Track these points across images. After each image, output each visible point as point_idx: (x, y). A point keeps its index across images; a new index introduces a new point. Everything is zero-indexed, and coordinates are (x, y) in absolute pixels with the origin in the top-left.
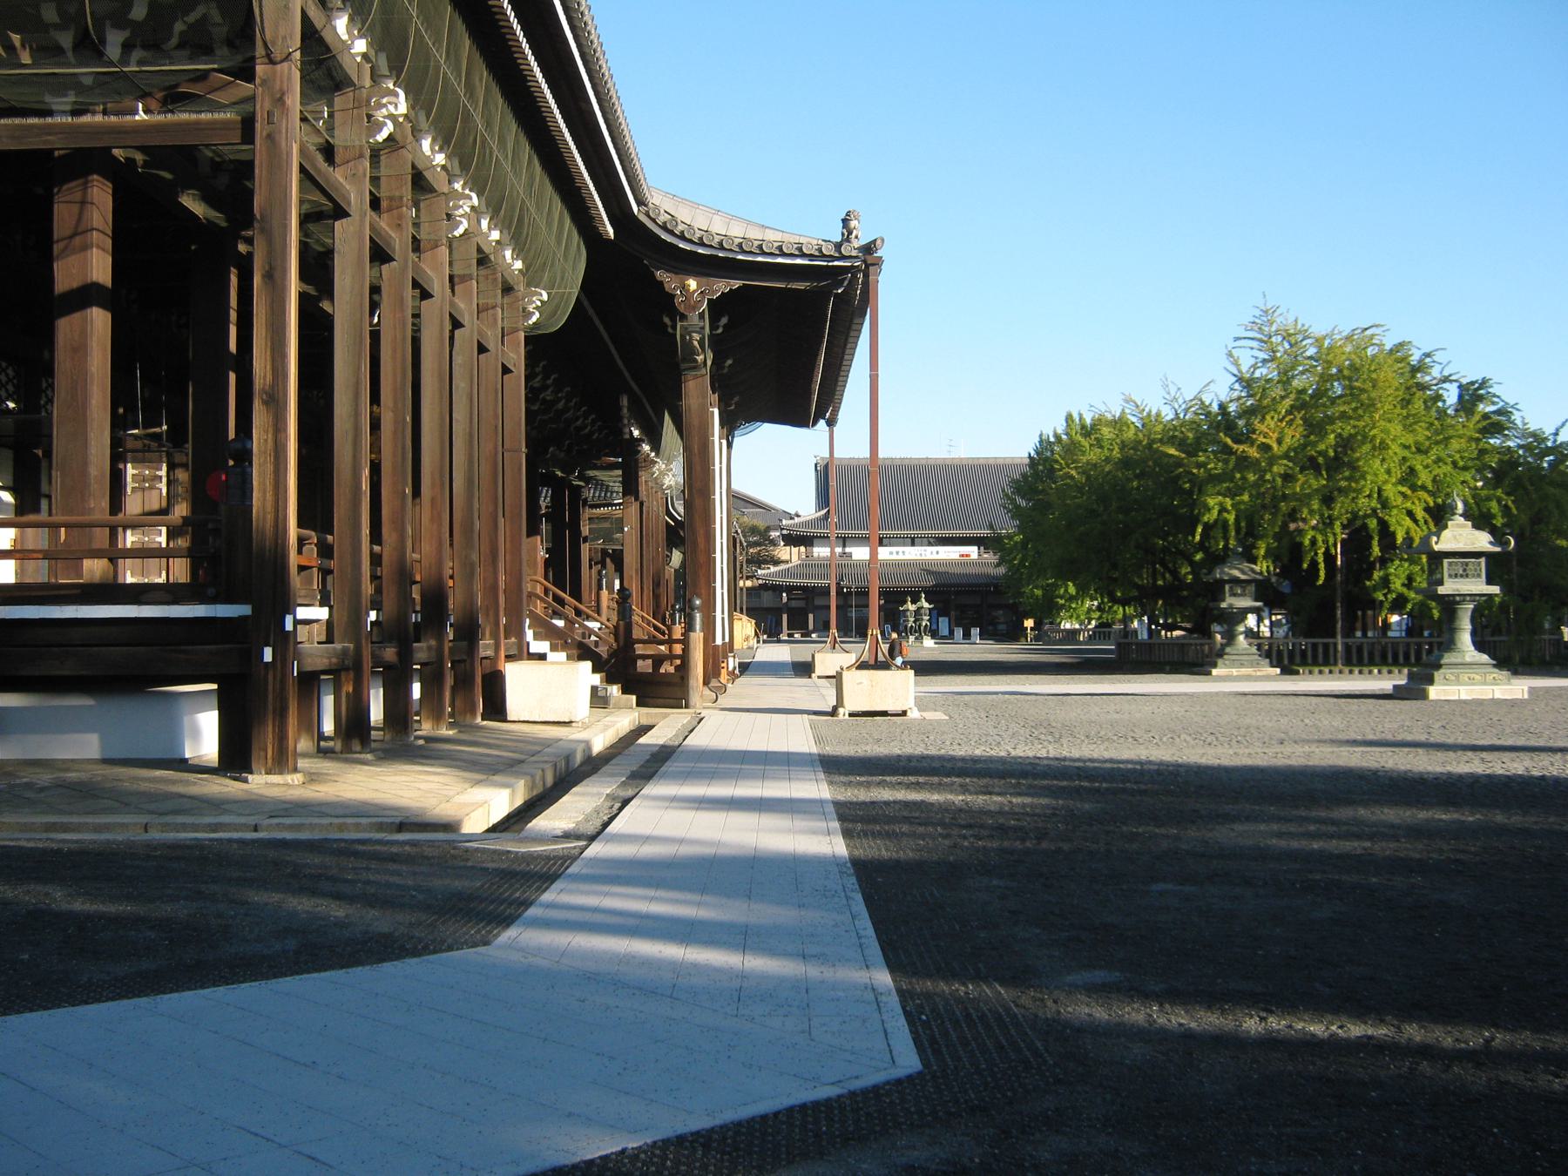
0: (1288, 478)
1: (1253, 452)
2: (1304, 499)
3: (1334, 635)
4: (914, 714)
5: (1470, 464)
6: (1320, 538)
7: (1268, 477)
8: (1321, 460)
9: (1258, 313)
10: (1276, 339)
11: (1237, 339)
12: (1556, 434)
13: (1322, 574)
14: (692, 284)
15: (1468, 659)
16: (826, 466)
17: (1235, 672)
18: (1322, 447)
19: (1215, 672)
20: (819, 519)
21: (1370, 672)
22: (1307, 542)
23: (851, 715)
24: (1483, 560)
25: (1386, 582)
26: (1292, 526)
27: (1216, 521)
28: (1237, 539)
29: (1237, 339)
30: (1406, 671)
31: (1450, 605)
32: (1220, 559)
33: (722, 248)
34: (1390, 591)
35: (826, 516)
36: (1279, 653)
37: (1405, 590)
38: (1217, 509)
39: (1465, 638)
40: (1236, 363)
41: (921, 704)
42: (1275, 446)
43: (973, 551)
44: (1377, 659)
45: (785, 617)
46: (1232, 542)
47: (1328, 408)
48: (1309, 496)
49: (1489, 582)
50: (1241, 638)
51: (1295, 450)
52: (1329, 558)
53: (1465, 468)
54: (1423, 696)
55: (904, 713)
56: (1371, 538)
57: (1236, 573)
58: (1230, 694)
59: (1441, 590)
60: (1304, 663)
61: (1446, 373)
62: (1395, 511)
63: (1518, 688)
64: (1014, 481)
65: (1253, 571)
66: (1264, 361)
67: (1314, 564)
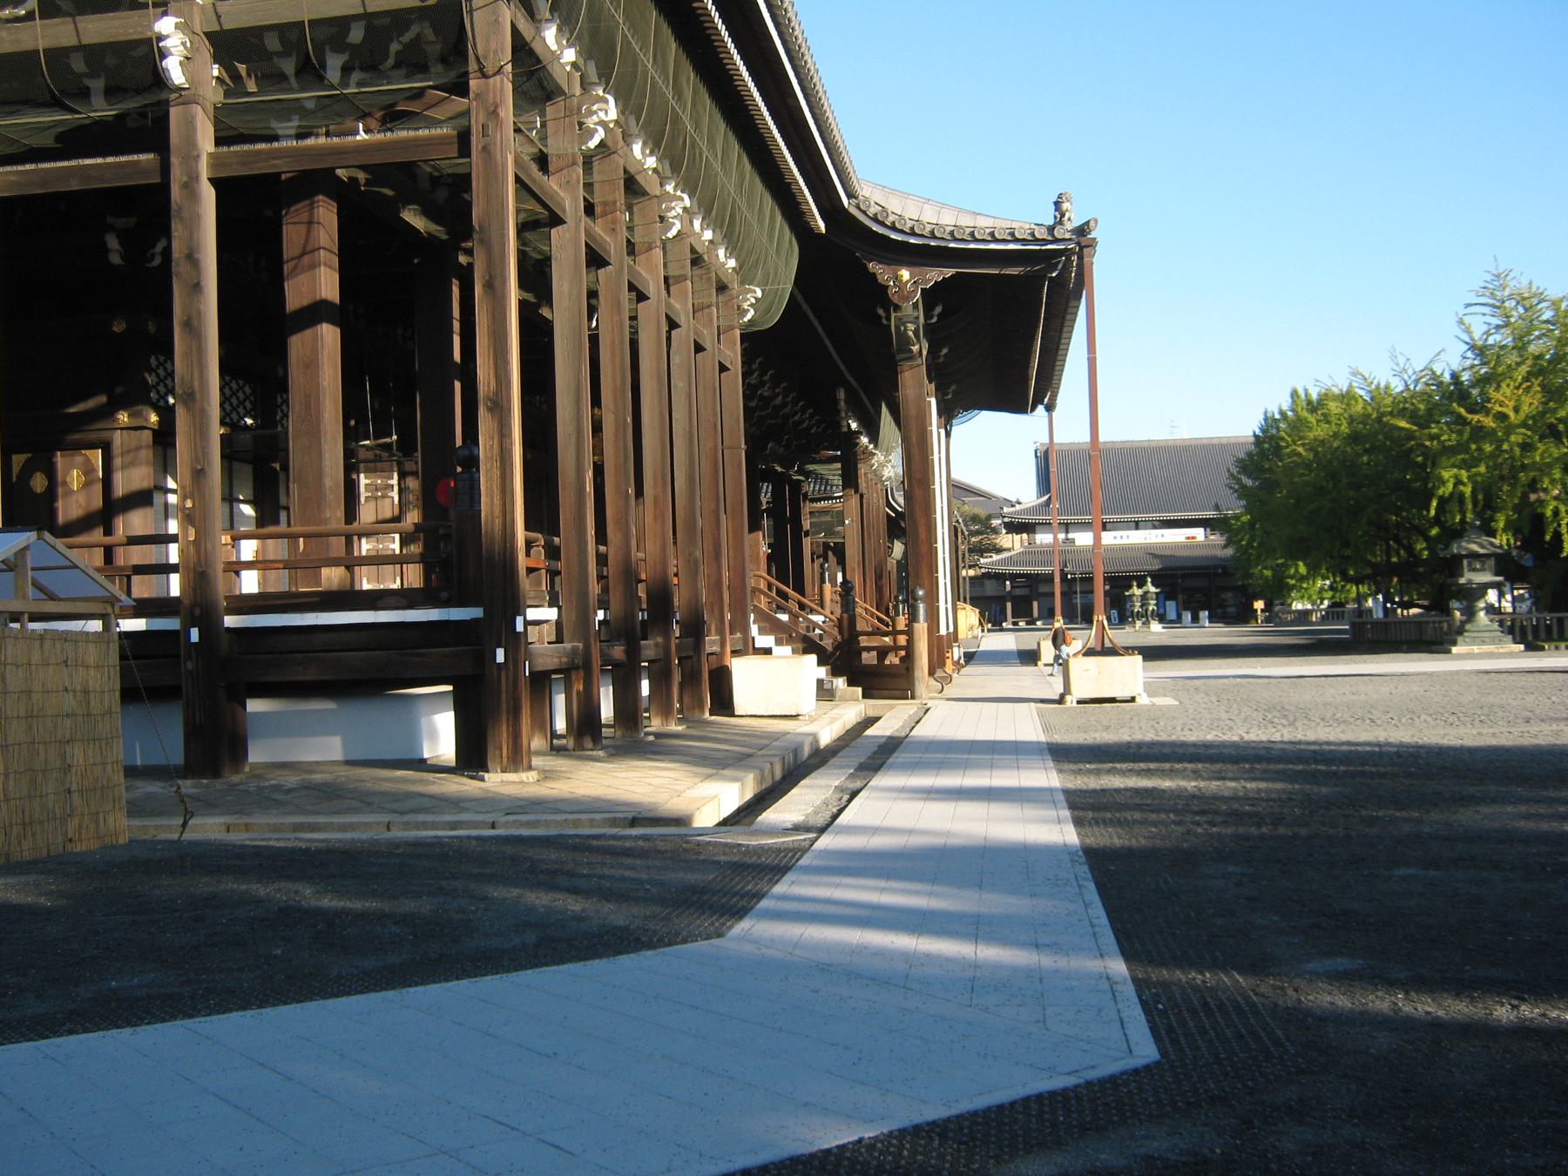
0: (1526, 447)
1: (1489, 422)
2: (1545, 469)
4: (1143, 700)
7: (1505, 446)
9: (1489, 278)
10: (1510, 304)
11: (1468, 305)
14: (905, 274)
16: (1046, 453)
17: (1476, 649)
19: (1455, 650)
20: (1041, 505)
22: (1549, 513)
27: (1452, 494)
28: (1474, 511)
29: (1468, 305)
32: (1457, 533)
33: (933, 237)
36: (1523, 630)
40: (1468, 331)
41: (1150, 689)
42: (1512, 415)
43: (1199, 534)
45: (1009, 605)
46: (1469, 516)
48: (1550, 466)
50: (1482, 614)
51: (1533, 418)
55: (1133, 700)
57: (1475, 547)
58: (1471, 672)
60: (1549, 639)
65: (1492, 544)
66: (1498, 327)
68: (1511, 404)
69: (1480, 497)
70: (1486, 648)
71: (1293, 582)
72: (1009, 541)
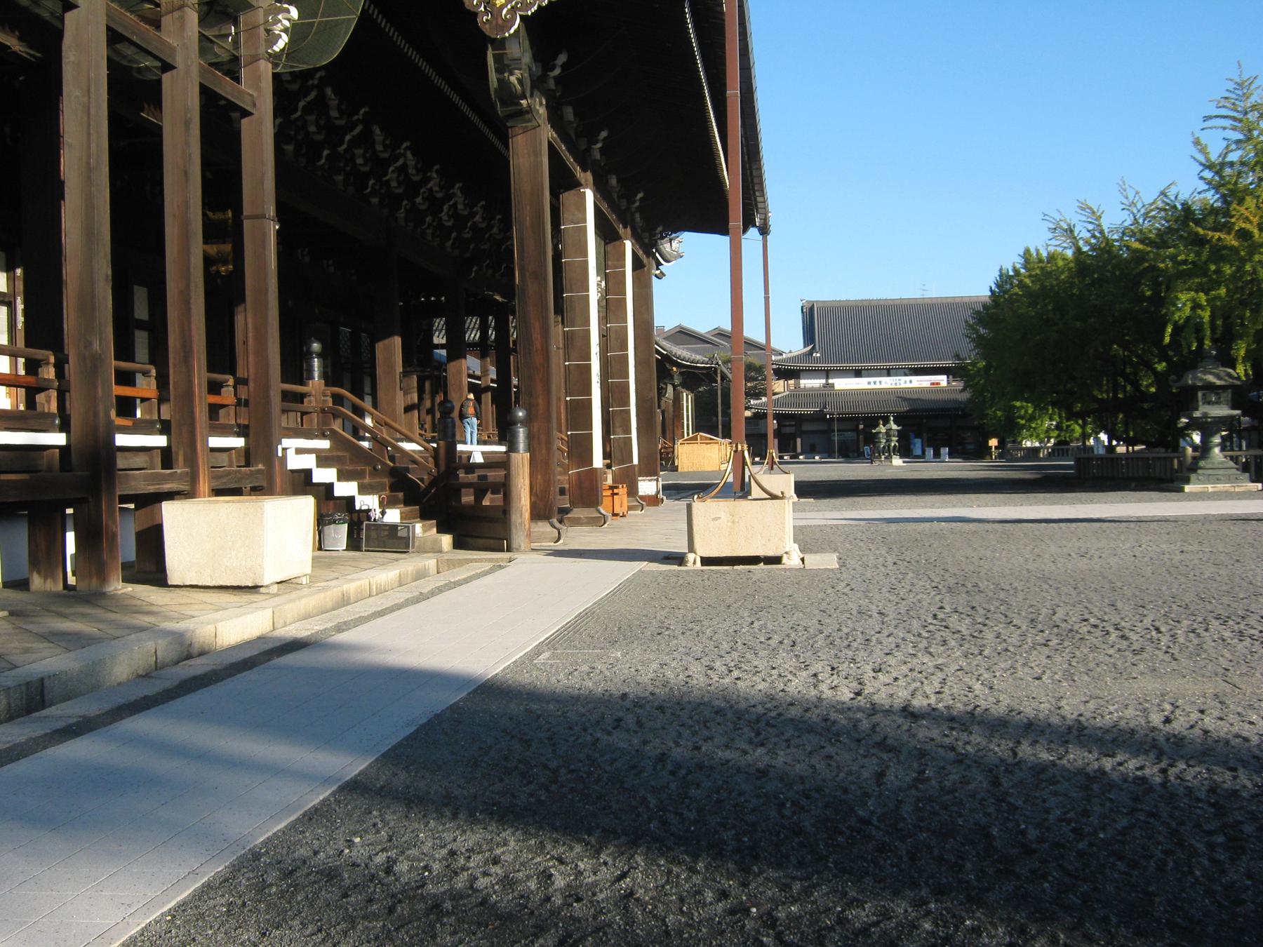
1: (1231, 240)
4: (793, 560)
7: (1248, 267)
9: (1231, 86)
16: (812, 309)
19: (1187, 488)
23: (706, 561)
27: (1188, 318)
28: (1214, 341)
32: (1196, 360)
35: (810, 353)
38: (1189, 304)
40: (1203, 150)
41: (807, 540)
43: (942, 380)
46: (1207, 343)
50: (1217, 450)
55: (777, 560)
57: (1211, 378)
64: (978, 312)
65: (1229, 375)
66: (1238, 142)
69: (1219, 323)
70: (1220, 487)
71: (1023, 422)
72: (779, 386)
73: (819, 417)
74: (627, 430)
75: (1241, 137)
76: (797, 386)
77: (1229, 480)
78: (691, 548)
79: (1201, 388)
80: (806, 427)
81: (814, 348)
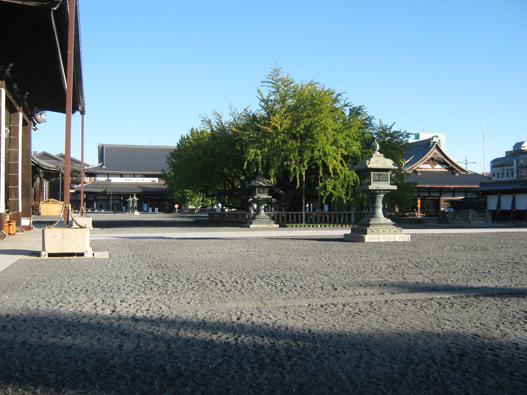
0: (284, 142)
1: (270, 130)
2: (291, 151)
3: (302, 211)
4: (89, 255)
5: (359, 138)
6: (297, 168)
7: (276, 141)
8: (298, 135)
9: (272, 70)
10: (279, 83)
11: (263, 82)
12: (391, 128)
13: (298, 184)
15: (382, 222)
16: (103, 148)
17: (260, 226)
18: (298, 129)
19: (251, 226)
20: (99, 167)
21: (317, 226)
22: (292, 170)
23: (50, 255)
24: (389, 173)
25: (325, 187)
26: (285, 163)
28: (262, 168)
29: (263, 82)
30: (351, 226)
31: (373, 194)
34: (326, 191)
35: (101, 166)
37: (333, 191)
38: (254, 154)
39: (380, 211)
40: (261, 94)
41: (96, 246)
42: (279, 127)
43: (156, 180)
44: (318, 220)
46: (260, 169)
47: (302, 114)
48: (294, 150)
49: (391, 184)
50: (263, 211)
51: (287, 130)
52: (301, 176)
53: (357, 140)
54: (362, 240)
55: (82, 254)
56: (319, 168)
57: (261, 183)
59: (370, 187)
60: (288, 222)
61: (346, 103)
62: (329, 157)
63: (403, 235)
64: (172, 153)
65: (268, 182)
66: (274, 92)
67: (295, 178)
68: (279, 123)
70: (263, 226)
72: (87, 180)
73: (104, 194)
74: (17, 197)
75: (275, 90)
76: (95, 180)
77: (267, 224)
78: (44, 249)
79: (257, 187)
80: (98, 198)
81: (103, 164)
